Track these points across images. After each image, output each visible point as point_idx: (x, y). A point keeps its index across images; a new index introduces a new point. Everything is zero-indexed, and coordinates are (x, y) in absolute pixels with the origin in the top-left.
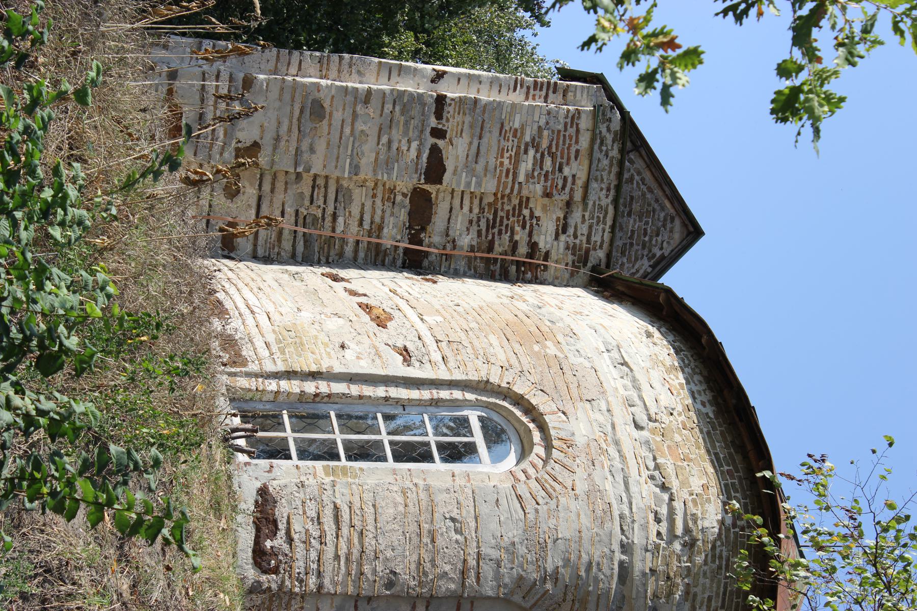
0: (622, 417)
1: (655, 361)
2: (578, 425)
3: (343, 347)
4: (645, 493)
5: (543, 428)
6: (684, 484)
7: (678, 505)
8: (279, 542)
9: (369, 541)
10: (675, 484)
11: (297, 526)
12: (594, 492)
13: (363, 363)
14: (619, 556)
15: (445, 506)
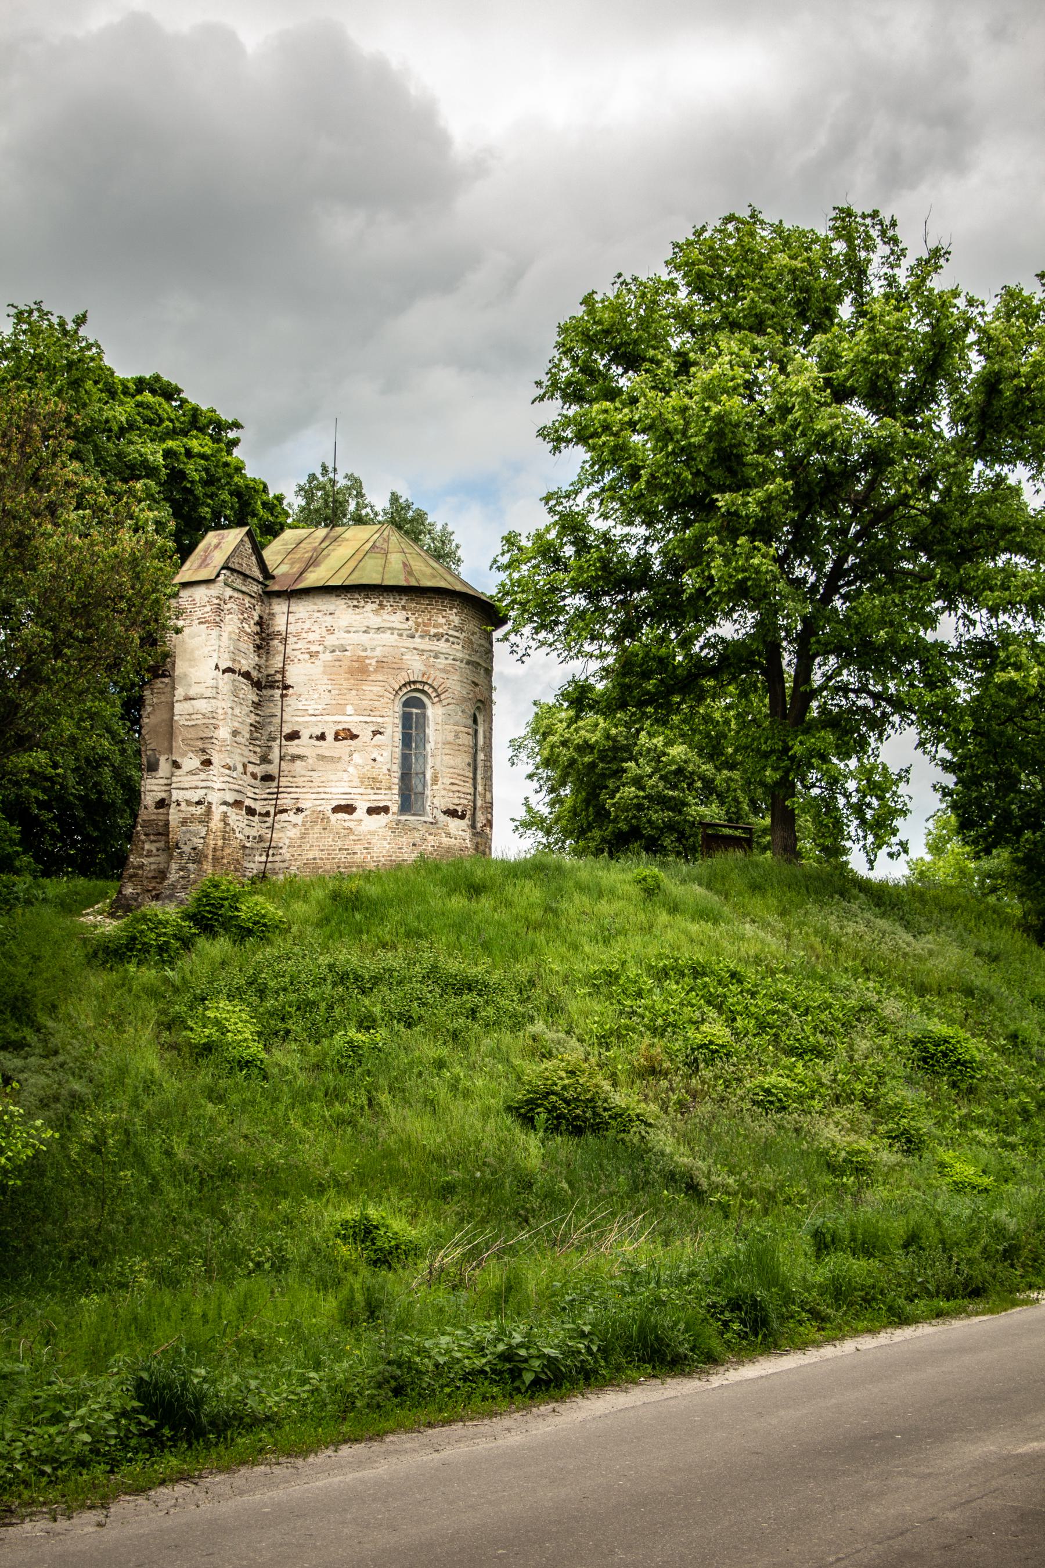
0: (410, 643)
1: (376, 612)
2: (415, 667)
3: (374, 760)
4: (442, 646)
5: (414, 682)
6: (441, 626)
7: (451, 632)
8: (459, 809)
9: (461, 772)
10: (441, 630)
11: (456, 801)
12: (444, 670)
13: (385, 754)
14: (463, 665)
15: (451, 737)
